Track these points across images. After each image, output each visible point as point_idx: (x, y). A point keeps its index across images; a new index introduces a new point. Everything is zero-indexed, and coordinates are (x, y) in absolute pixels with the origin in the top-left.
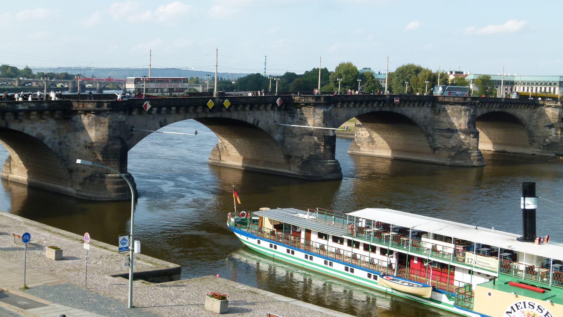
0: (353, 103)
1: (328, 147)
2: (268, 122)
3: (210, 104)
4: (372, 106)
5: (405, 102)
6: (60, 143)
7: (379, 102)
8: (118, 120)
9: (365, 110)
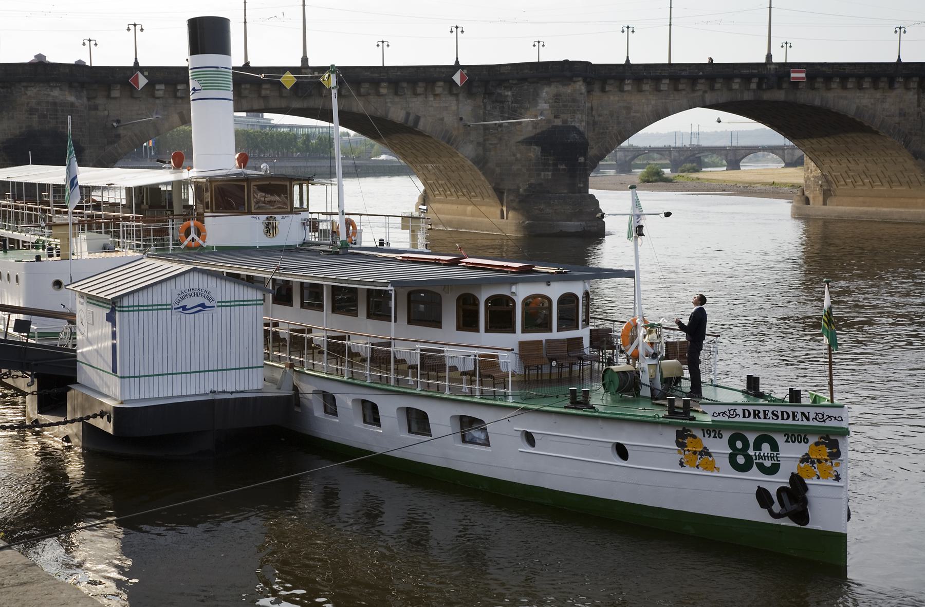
1: (563, 167)
2: (442, 119)
8: (50, 99)
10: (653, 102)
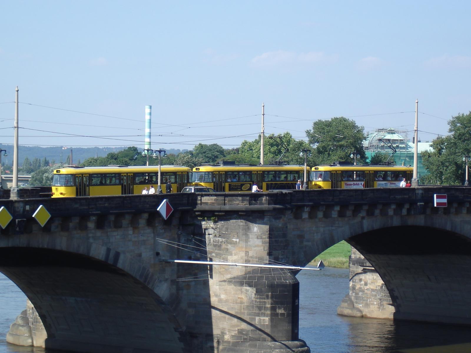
0: (337, 208)
1: (280, 311)
2: (140, 255)
4: (384, 213)
5: (461, 204)
7: (400, 205)
9: (368, 224)
10: (322, 229)
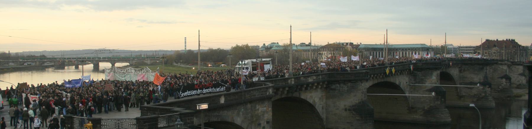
3: (387, 71)
6: (323, 108)
